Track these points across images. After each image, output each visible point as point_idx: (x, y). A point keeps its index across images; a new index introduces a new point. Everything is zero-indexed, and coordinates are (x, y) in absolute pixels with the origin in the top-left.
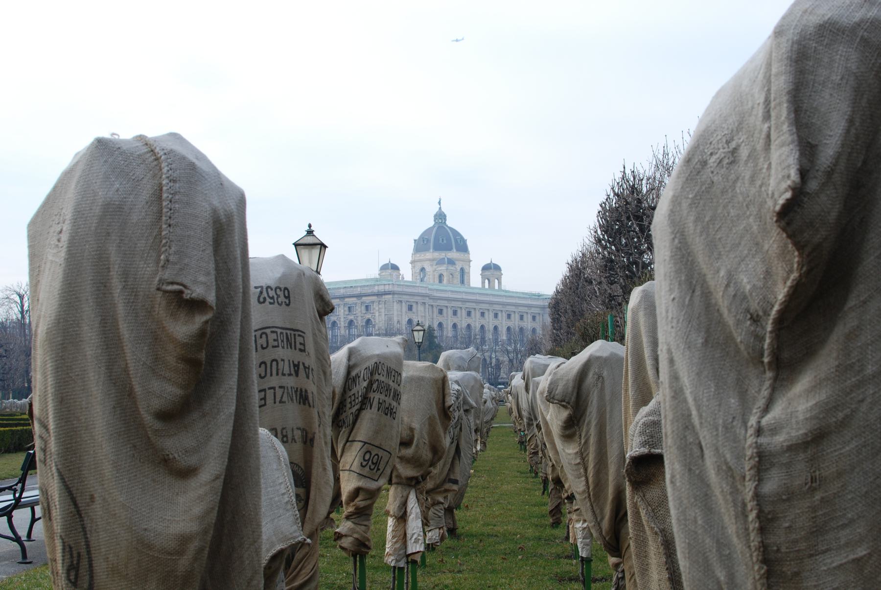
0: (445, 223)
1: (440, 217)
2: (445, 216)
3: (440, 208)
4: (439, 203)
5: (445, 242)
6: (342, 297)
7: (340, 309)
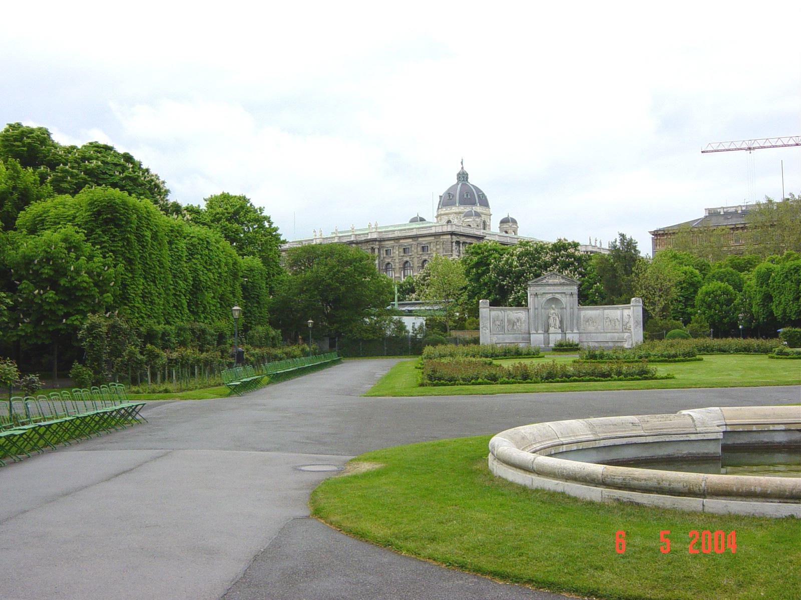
0: (467, 180)
1: (463, 176)
2: (467, 174)
3: (462, 168)
4: (462, 163)
5: (469, 197)
6: (397, 239)
7: (394, 251)
